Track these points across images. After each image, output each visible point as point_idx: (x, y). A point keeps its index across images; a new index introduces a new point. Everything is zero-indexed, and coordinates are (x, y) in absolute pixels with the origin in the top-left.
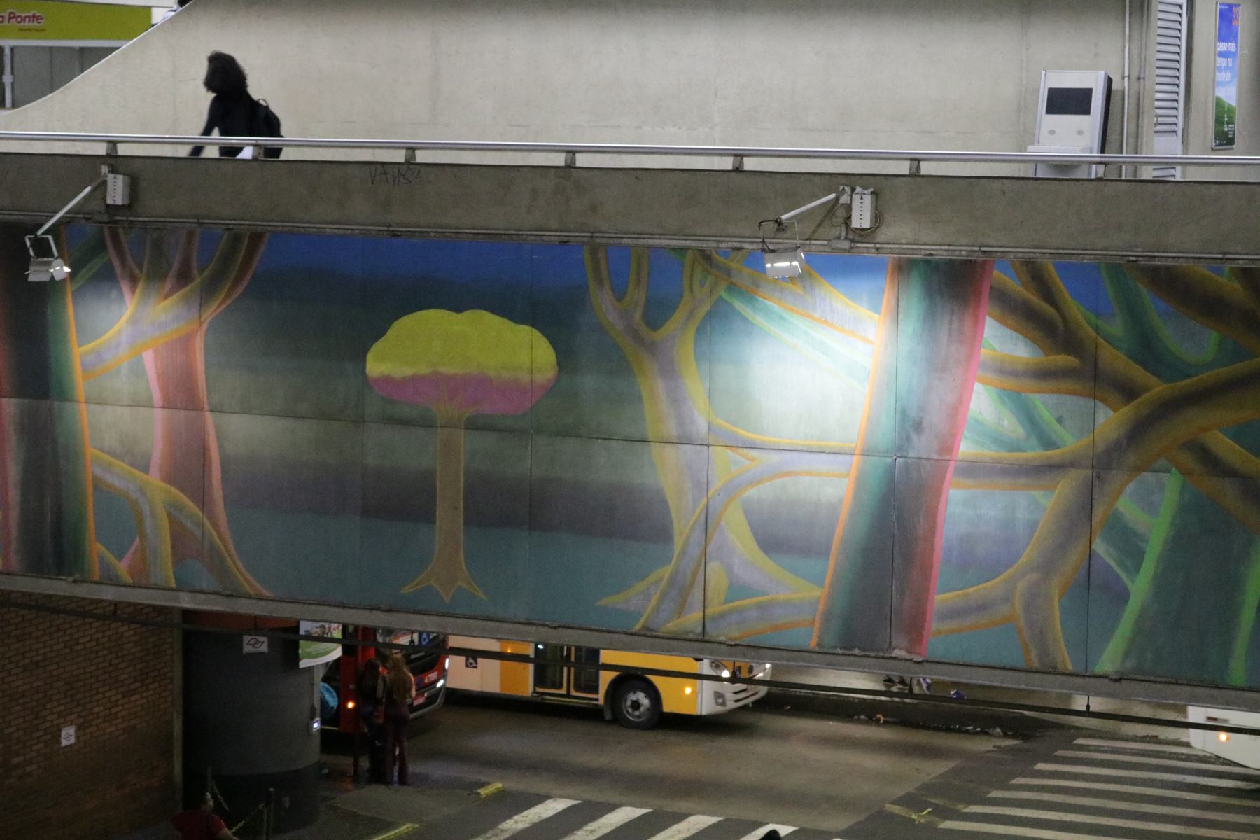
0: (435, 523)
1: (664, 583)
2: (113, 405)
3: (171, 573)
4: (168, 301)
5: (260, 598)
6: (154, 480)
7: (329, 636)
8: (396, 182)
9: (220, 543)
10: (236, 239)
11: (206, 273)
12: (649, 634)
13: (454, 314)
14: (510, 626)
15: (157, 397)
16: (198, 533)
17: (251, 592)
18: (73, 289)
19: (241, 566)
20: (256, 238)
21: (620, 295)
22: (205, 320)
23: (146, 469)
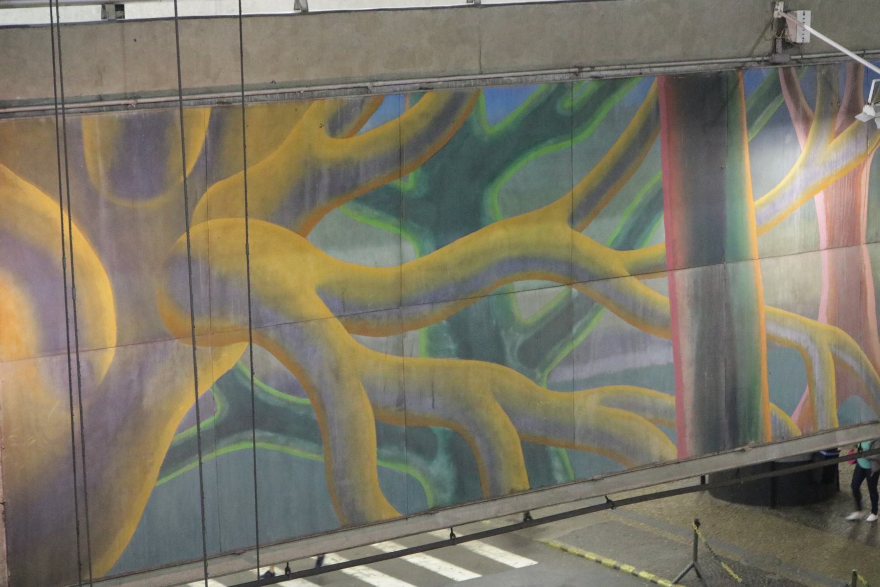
2: (785, 256)
4: (839, 138)
6: (822, 323)
16: (856, 368)
22: (871, 152)
23: (815, 316)
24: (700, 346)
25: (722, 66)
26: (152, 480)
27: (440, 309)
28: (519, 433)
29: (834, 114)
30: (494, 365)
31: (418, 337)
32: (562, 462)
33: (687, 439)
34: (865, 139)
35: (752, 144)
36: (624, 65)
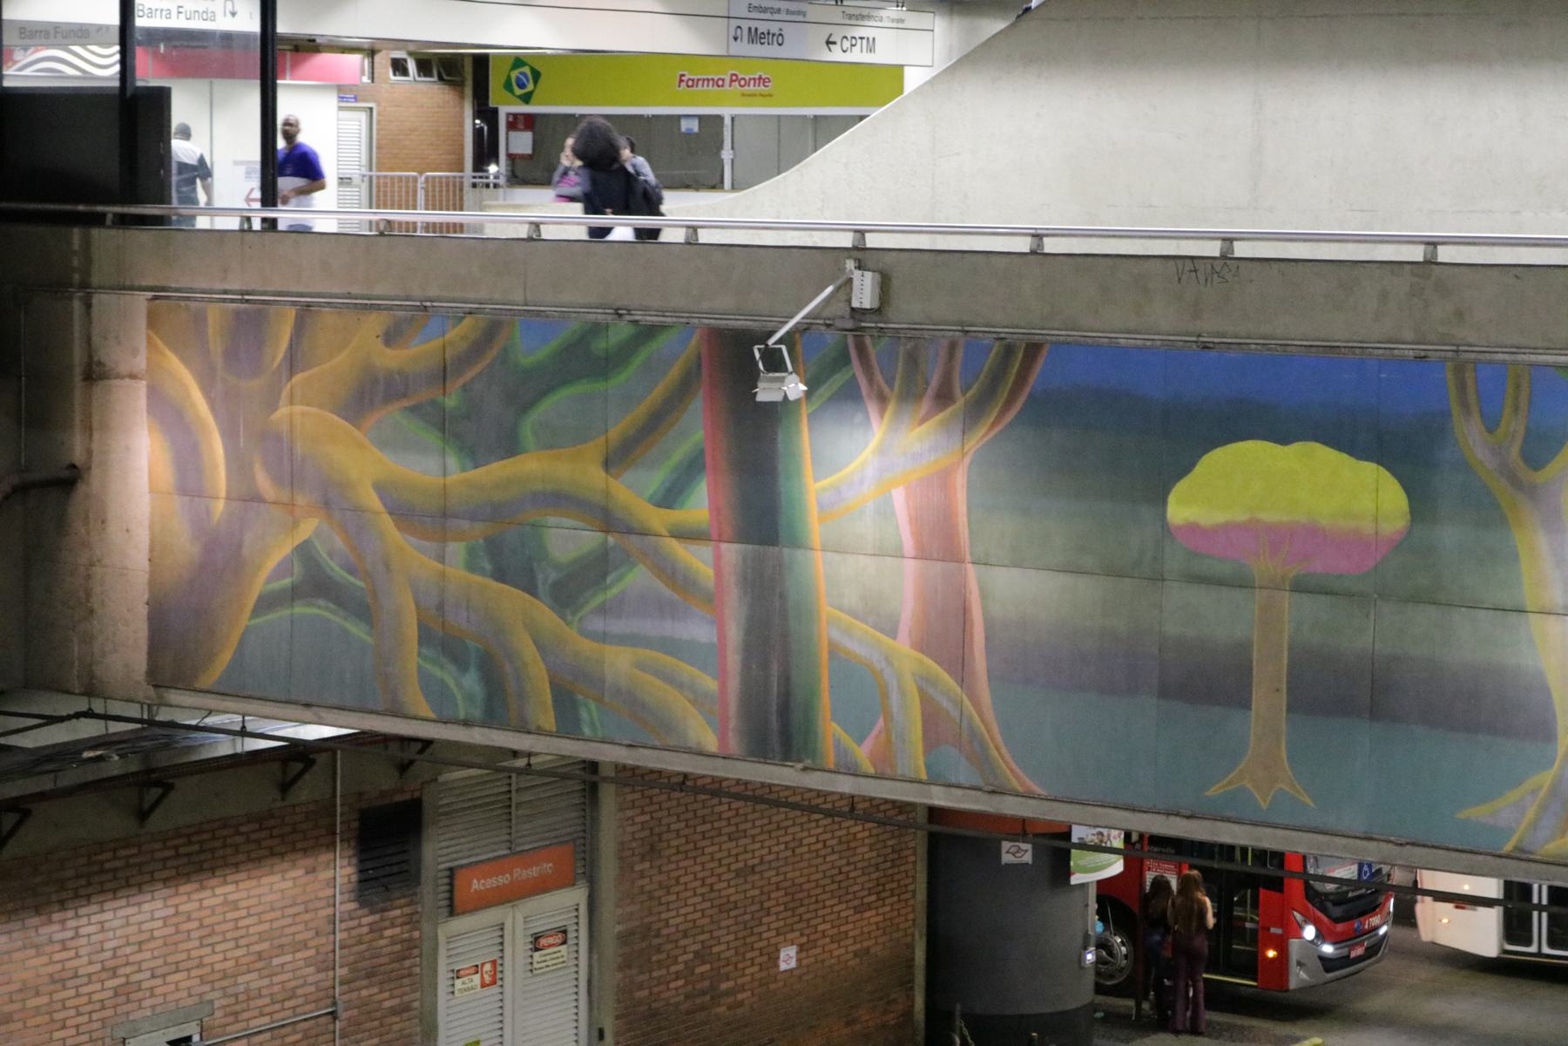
0: (1249, 708)
1: (1542, 794)
3: (921, 762)
4: (925, 426)
5: (1029, 796)
7: (1109, 845)
8: (1209, 280)
9: (983, 728)
10: (1009, 351)
11: (969, 394)
12: (1525, 856)
13: (1279, 446)
14: (1343, 841)
15: (908, 545)
16: (955, 714)
17: (1020, 789)
18: (810, 411)
19: (1008, 757)
20: (1033, 349)
21: (1491, 425)
22: (969, 450)
23: (893, 633)
24: (748, 632)
25: (756, 324)
26: (245, 620)
27: (479, 527)
28: (548, 670)
29: (918, 397)
30: (527, 596)
31: (456, 550)
32: (590, 713)
33: (730, 734)
34: (960, 433)
35: (811, 416)
36: (662, 312)
